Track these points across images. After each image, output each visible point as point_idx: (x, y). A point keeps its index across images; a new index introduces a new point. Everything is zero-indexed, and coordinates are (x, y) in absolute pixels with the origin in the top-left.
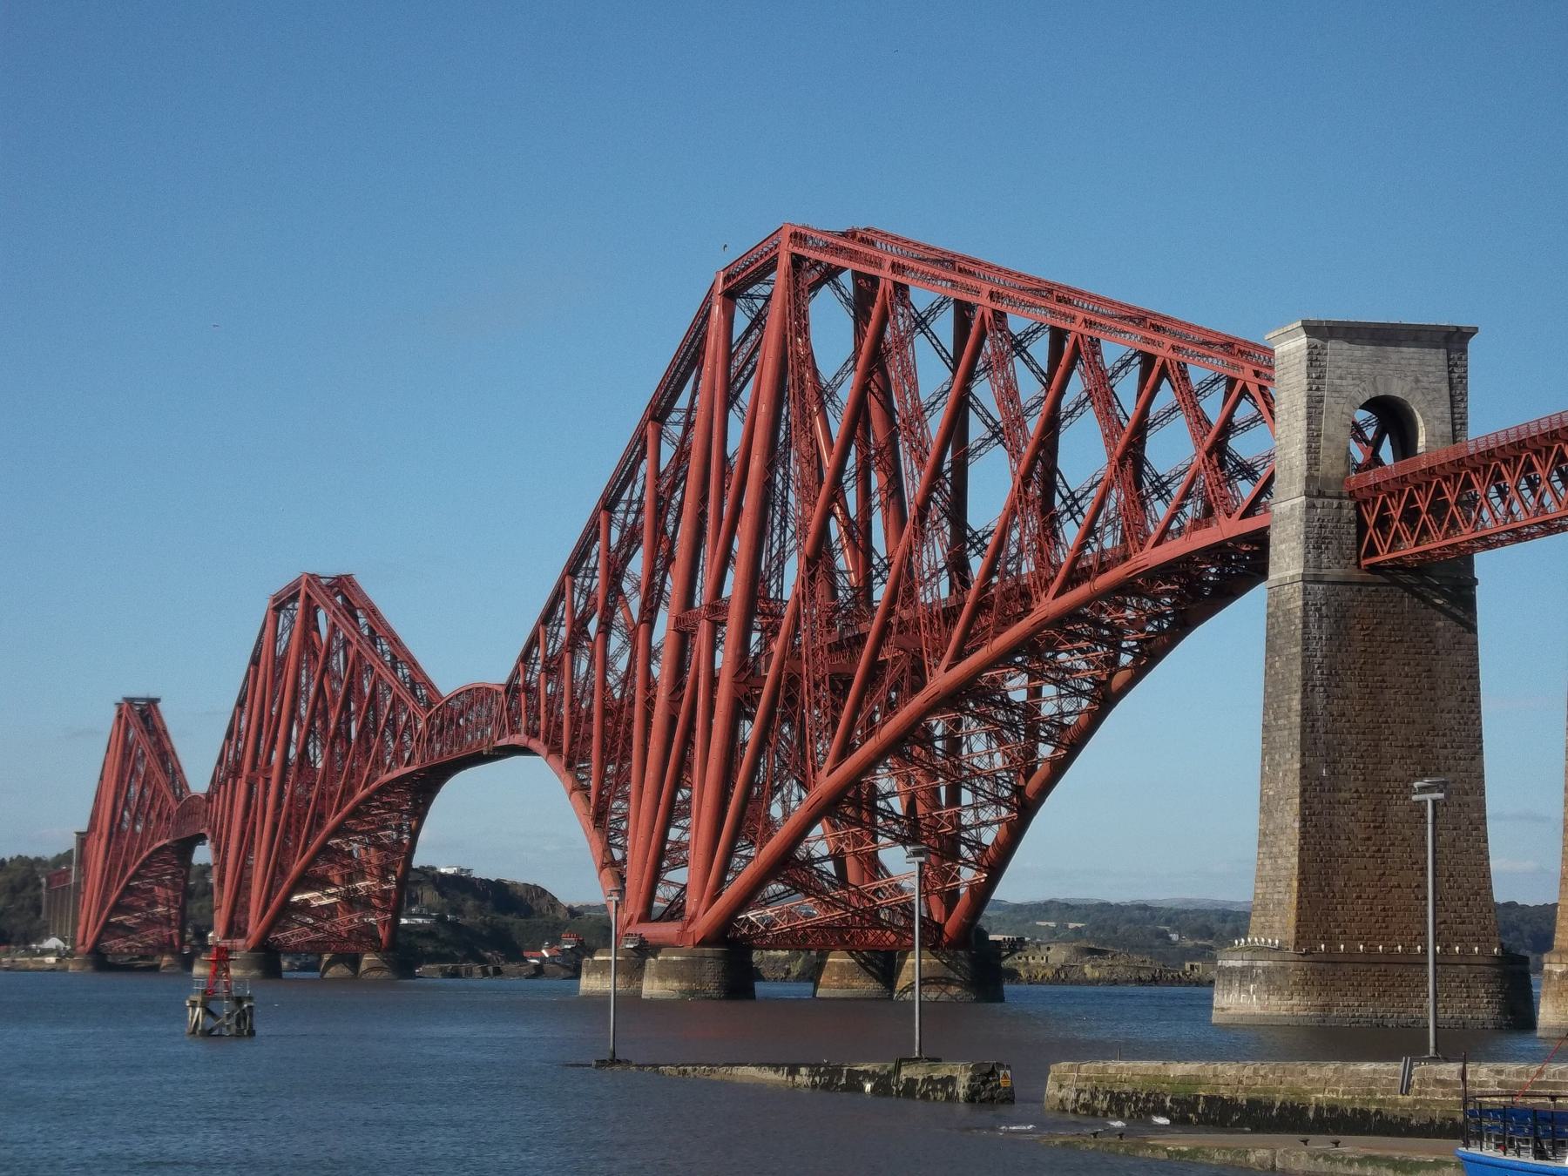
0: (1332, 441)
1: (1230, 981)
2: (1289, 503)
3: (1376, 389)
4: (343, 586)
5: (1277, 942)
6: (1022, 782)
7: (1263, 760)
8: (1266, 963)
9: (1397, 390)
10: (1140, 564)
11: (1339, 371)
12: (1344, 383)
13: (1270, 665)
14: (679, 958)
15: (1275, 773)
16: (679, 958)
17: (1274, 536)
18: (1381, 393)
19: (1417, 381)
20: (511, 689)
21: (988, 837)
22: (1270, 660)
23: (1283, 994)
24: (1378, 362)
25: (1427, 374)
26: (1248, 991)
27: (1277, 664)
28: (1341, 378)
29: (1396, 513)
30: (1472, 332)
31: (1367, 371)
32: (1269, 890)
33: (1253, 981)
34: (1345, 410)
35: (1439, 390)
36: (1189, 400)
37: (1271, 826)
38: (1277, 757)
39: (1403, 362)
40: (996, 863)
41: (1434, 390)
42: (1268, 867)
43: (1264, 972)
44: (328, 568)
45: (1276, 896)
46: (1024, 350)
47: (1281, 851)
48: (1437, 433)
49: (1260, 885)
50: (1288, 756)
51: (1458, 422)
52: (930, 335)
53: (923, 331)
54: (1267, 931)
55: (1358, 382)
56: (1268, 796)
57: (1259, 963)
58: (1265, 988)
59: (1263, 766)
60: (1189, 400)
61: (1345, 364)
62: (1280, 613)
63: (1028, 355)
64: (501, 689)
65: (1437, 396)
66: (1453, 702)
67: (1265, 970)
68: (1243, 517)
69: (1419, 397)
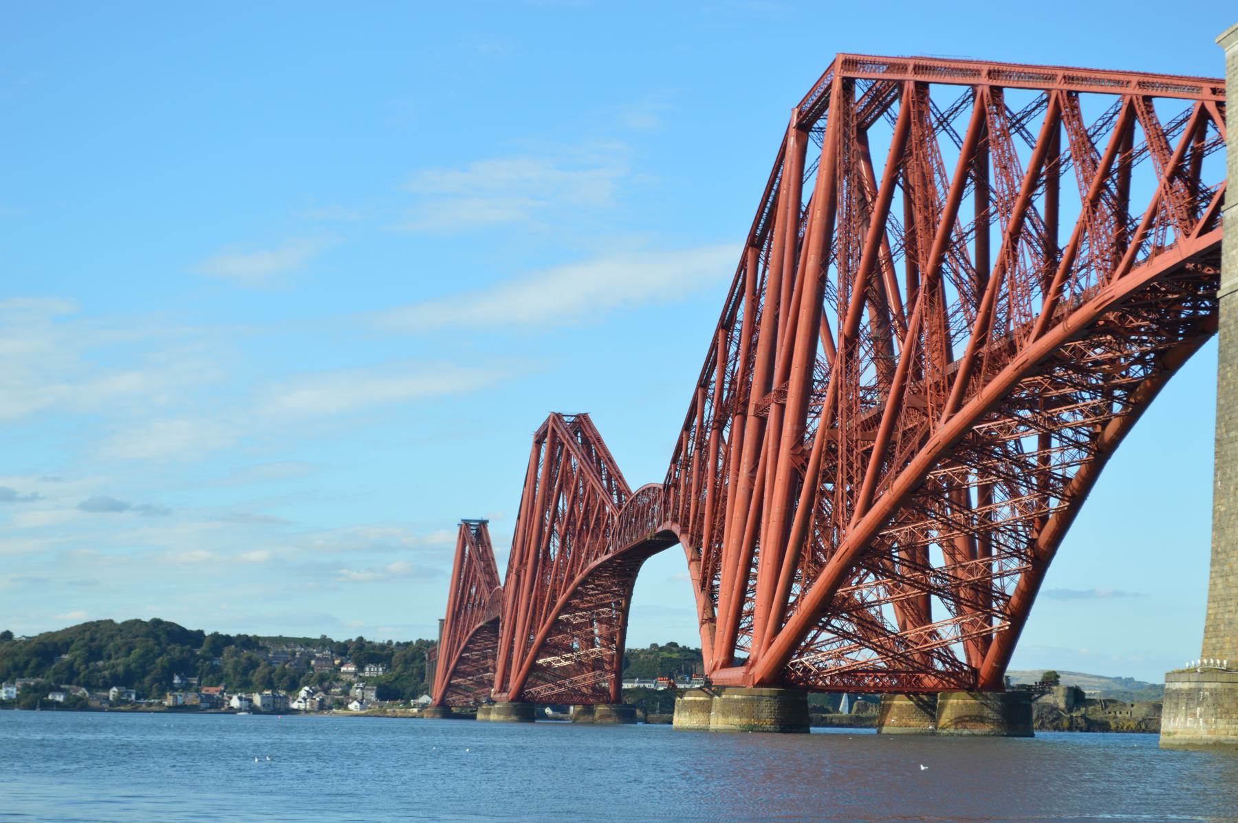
1: (1177, 704)
5: (1225, 662)
6: (1035, 535)
7: (1216, 475)
8: (1213, 685)
10: (1106, 297)
13: (1222, 377)
14: (740, 697)
16: (740, 697)
20: (667, 488)
22: (1222, 372)
23: (1231, 718)
26: (1195, 714)
27: (1229, 375)
32: (1221, 610)
33: (1199, 704)
37: (1223, 544)
38: (1228, 470)
42: (1220, 586)
43: (1211, 694)
45: (1227, 616)
46: (1023, 127)
47: (1232, 569)
49: (1212, 605)
52: (951, 133)
53: (944, 128)
54: (1218, 653)
56: (1220, 512)
57: (1207, 685)
58: (1212, 711)
59: (1215, 482)
62: (1232, 321)
63: (1027, 132)
64: (661, 487)
67: (1214, 693)
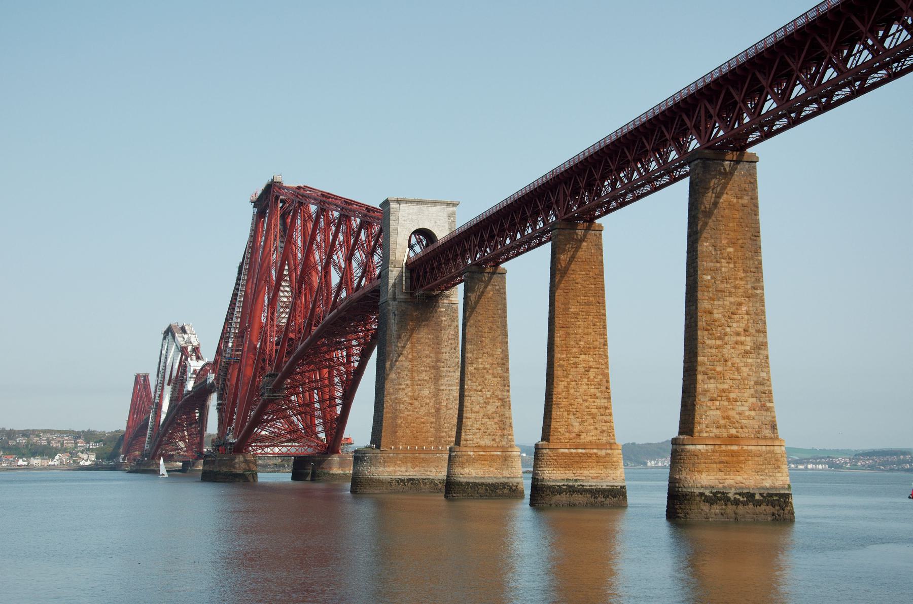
0: (401, 246)
3: (419, 225)
11: (403, 218)
12: (406, 223)
15: (379, 378)
18: (421, 227)
19: (435, 222)
21: (339, 409)
24: (419, 214)
25: (439, 220)
28: (404, 221)
31: (416, 219)
34: (406, 233)
35: (444, 226)
39: (430, 215)
41: (442, 226)
55: (411, 222)
57: (367, 455)
65: (443, 228)
66: (448, 350)
68: (378, 279)
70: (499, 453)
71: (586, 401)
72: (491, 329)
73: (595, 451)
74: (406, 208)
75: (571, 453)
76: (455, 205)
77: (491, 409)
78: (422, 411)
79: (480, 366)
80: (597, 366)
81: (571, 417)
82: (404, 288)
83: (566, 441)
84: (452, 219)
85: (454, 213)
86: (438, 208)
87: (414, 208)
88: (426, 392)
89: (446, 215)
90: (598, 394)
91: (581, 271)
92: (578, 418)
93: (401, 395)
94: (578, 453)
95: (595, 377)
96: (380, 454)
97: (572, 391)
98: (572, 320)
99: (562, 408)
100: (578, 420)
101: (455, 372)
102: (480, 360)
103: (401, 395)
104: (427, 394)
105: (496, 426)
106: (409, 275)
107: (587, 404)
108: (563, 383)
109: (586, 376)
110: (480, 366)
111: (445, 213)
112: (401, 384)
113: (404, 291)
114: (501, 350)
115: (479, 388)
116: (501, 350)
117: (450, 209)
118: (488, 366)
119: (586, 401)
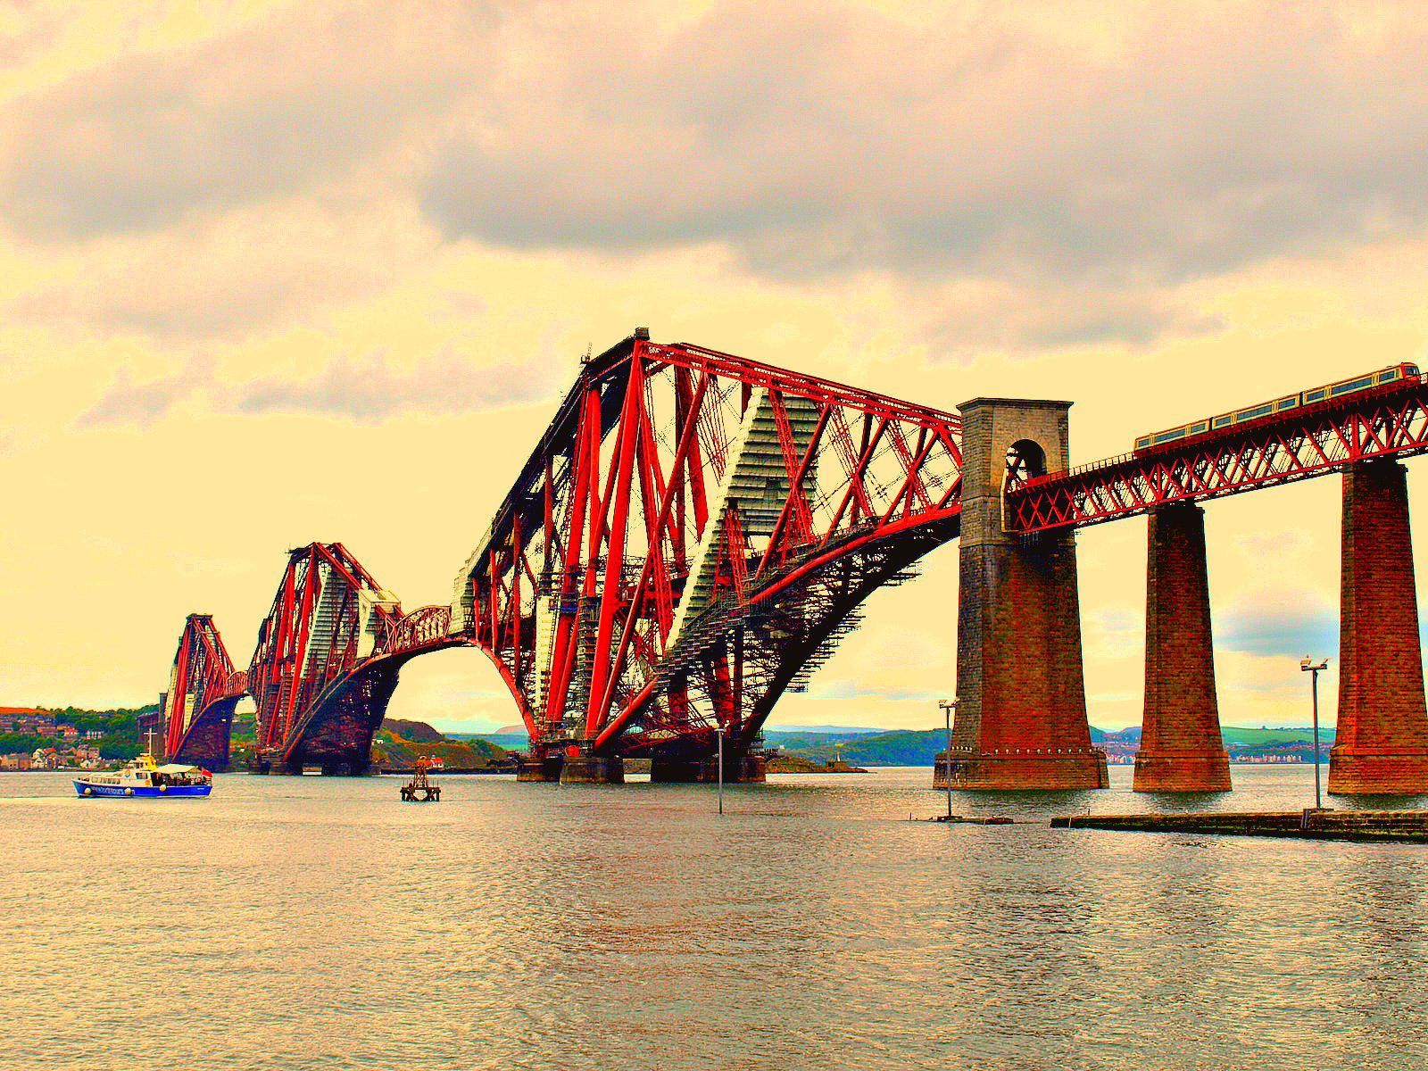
2: (972, 502)
4: (337, 548)
9: (1031, 436)
15: (967, 653)
17: (963, 518)
29: (1035, 506)
30: (1071, 404)
36: (899, 443)
40: (764, 706)
41: (1051, 436)
44: (326, 540)
48: (1054, 461)
50: (975, 643)
51: (1064, 454)
57: (961, 761)
60: (899, 443)
61: (1003, 421)
67: (966, 766)
69: (1043, 440)
70: (1203, 759)
71: (1395, 694)
72: (1187, 590)
73: (1408, 757)
74: (1002, 412)
75: (1381, 761)
76: (1065, 406)
77: (1191, 700)
78: (1034, 699)
79: (1176, 642)
80: (1407, 649)
81: (1379, 714)
82: (1003, 525)
83: (1374, 745)
84: (1064, 425)
85: (1066, 417)
86: (1046, 411)
87: (1014, 411)
88: (1037, 672)
89: (1054, 420)
90: (1410, 685)
91: (1383, 526)
92: (1385, 715)
93: (1004, 677)
94: (1388, 761)
95: (1405, 664)
96: (979, 761)
97: (1379, 682)
98: (1375, 590)
99: (1367, 703)
100: (1387, 718)
101: (1074, 644)
102: (1176, 634)
103: (1004, 677)
104: (1037, 676)
105: (1200, 722)
106: (1007, 506)
107: (1396, 697)
108: (1367, 671)
109: (1395, 662)
110: (1176, 642)
111: (1054, 417)
112: (1003, 663)
113: (1003, 530)
114: (1201, 620)
115: (1176, 672)
116: (1201, 620)
117: (1061, 413)
118: (1185, 642)
119: (1395, 694)
